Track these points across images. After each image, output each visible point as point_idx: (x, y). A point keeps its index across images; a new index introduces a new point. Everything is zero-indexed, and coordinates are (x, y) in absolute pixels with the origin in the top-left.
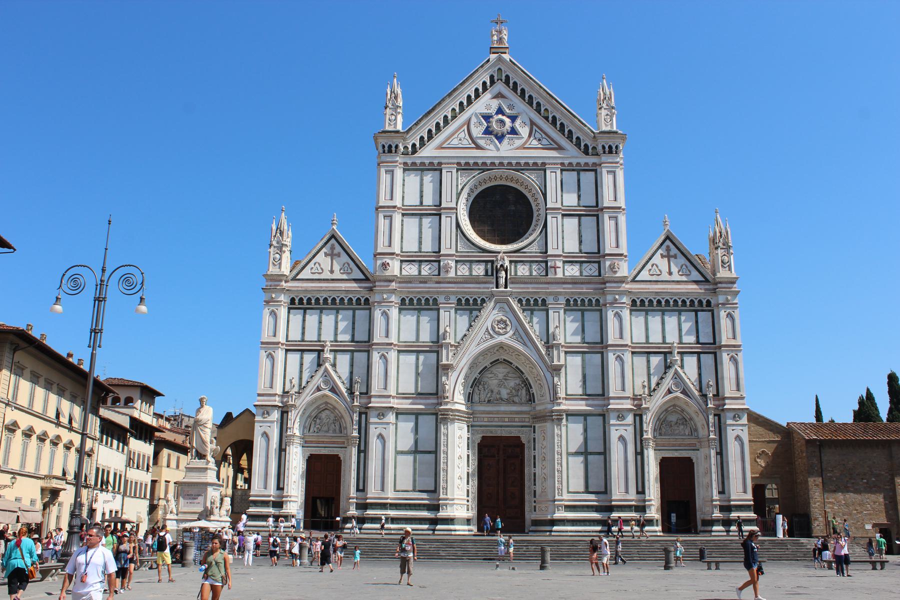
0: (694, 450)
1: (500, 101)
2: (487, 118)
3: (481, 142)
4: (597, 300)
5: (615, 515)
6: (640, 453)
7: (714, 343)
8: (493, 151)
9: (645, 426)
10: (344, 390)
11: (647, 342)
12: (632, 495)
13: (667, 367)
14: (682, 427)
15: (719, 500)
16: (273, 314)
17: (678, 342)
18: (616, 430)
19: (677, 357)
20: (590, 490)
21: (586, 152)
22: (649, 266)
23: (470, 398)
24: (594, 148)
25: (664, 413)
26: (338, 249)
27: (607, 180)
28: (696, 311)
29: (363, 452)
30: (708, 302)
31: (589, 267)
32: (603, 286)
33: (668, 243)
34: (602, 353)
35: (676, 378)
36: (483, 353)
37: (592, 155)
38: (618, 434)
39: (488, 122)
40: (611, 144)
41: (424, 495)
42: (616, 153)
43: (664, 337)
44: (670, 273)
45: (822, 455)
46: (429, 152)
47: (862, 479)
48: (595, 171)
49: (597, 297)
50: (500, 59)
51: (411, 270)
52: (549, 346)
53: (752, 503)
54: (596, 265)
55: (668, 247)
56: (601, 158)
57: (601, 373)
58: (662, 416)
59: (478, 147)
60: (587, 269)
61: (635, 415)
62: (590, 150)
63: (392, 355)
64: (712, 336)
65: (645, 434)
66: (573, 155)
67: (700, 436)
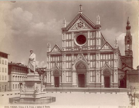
1: (80, 21)
2: (78, 24)
3: (78, 28)
5: (97, 85)
6: (101, 76)
8: (80, 29)
10: (59, 68)
11: (103, 59)
12: (99, 82)
13: (106, 63)
16: (48, 57)
19: (107, 62)
23: (77, 69)
24: (95, 28)
26: (57, 47)
27: (97, 33)
28: (111, 54)
29: (61, 76)
30: (113, 53)
36: (78, 62)
39: (78, 24)
41: (70, 82)
46: (70, 31)
50: (80, 13)
51: (67, 50)
52: (88, 61)
59: (77, 29)
63: (65, 63)
66: (92, 29)
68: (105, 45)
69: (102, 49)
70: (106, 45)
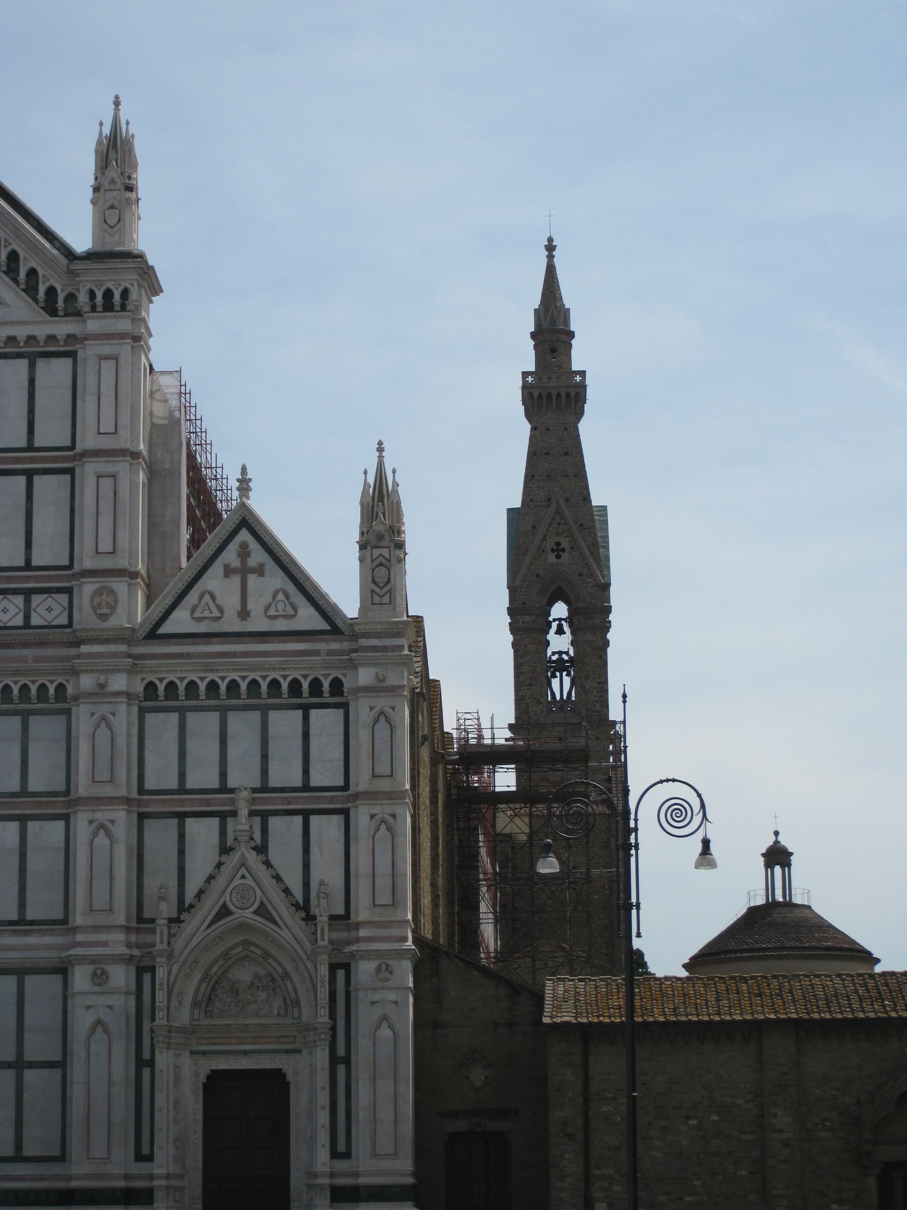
0: (288, 1052)
4: (61, 687)
7: (346, 787)
9: (161, 996)
13: (225, 850)
14: (264, 995)
15: (332, 1175)
17: (257, 784)
18: (88, 1008)
20: (27, 1152)
21: (50, 308)
22: (192, 598)
25: (221, 962)
28: (306, 709)
30: (337, 686)
31: (46, 605)
32: (73, 651)
33: (244, 535)
34: (66, 818)
35: (243, 877)
37: (66, 315)
38: (90, 1019)
40: (110, 285)
42: (123, 308)
43: (223, 775)
44: (244, 614)
45: (591, 1060)
47: (688, 1118)
48: (72, 355)
49: (59, 680)
53: (410, 1180)
54: (64, 598)
55: (244, 546)
56: (85, 322)
57: (62, 867)
58: (214, 969)
60: (42, 610)
61: (140, 971)
62: (60, 303)
64: (342, 770)
65: (160, 1015)
67: (305, 1018)
68: (217, 568)
69: (167, 628)
70: (228, 571)
